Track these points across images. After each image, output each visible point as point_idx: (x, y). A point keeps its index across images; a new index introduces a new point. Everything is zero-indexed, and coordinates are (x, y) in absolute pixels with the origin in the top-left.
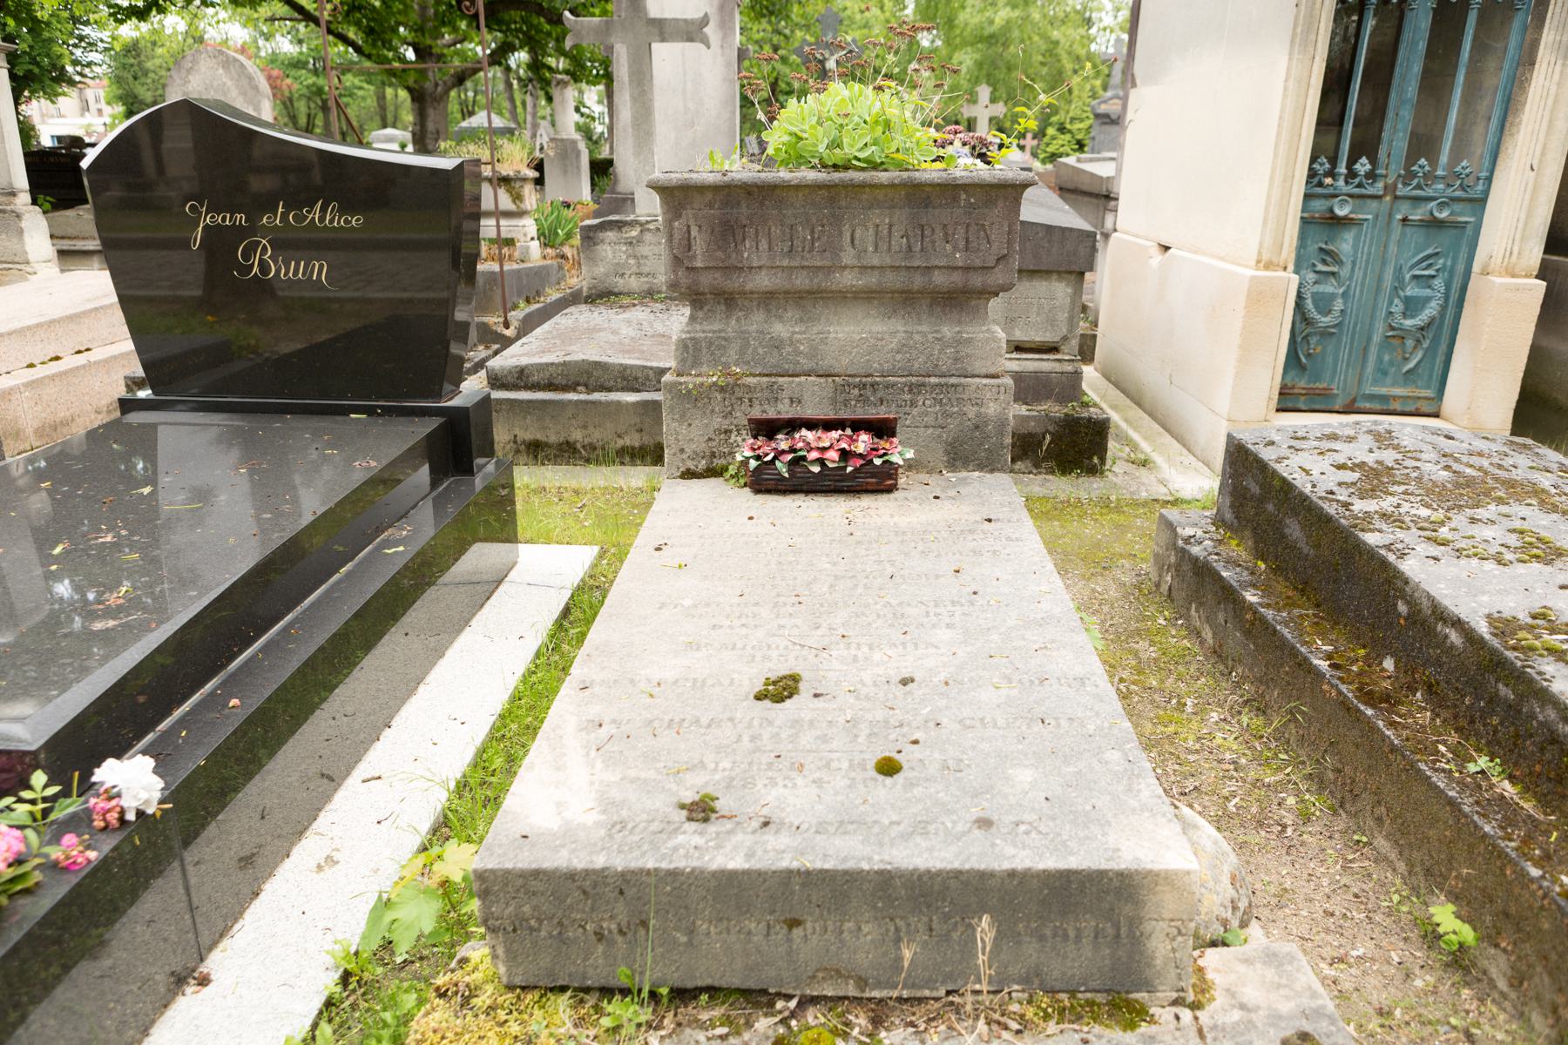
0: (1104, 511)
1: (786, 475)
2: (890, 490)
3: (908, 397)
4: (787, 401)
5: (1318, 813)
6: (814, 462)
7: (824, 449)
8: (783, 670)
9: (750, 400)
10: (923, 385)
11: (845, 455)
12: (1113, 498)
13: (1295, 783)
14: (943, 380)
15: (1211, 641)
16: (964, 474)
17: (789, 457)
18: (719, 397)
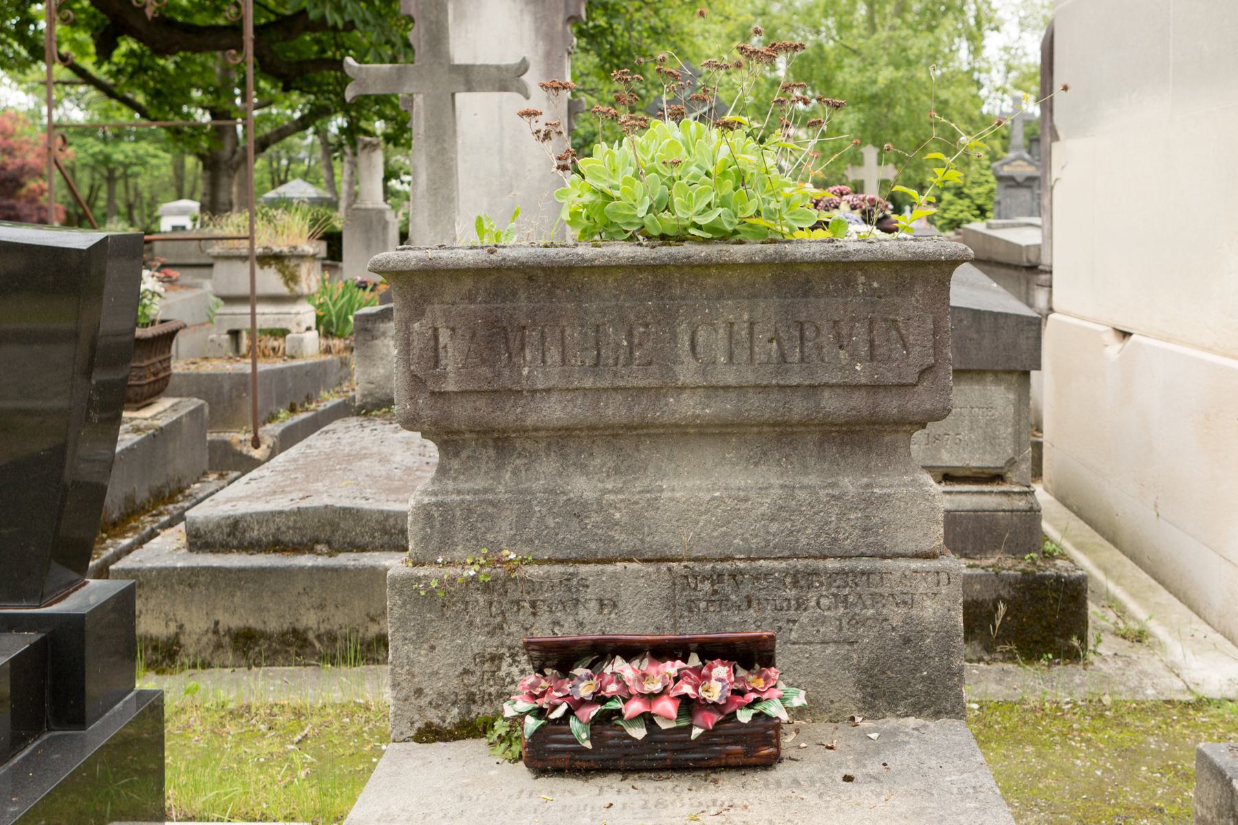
0: (1099, 723)
1: (588, 745)
2: (768, 764)
3: (791, 593)
4: (593, 604)
7: (652, 697)
9: (533, 604)
10: (816, 573)
11: (688, 706)
12: (1107, 700)
14: (847, 564)
16: (891, 722)
17: (593, 711)
18: (481, 599)
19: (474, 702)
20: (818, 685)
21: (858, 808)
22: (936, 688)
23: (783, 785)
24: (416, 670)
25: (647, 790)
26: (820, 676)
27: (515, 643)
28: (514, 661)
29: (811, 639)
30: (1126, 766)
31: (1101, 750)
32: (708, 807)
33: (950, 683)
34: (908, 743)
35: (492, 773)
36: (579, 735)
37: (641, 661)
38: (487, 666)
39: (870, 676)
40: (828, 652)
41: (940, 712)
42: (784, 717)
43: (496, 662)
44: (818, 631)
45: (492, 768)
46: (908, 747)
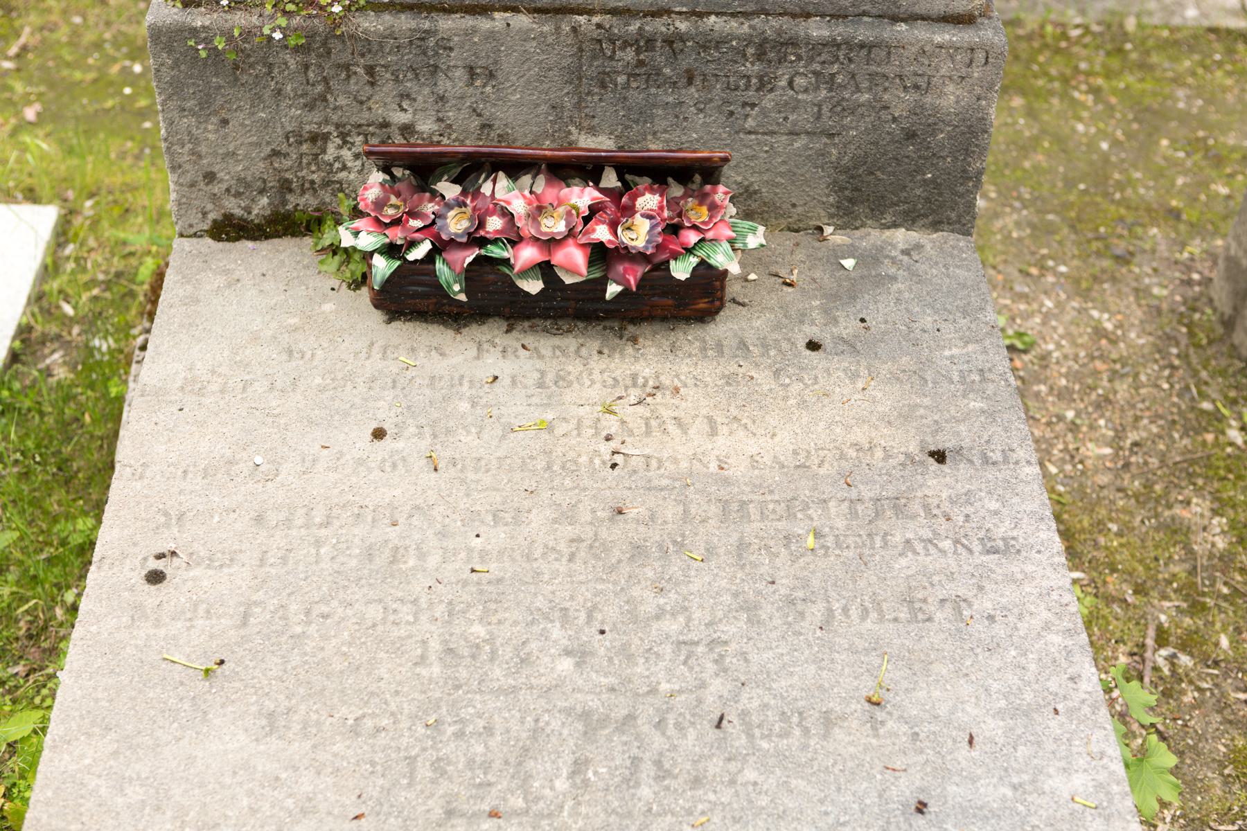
0: (1115, 63)
1: (463, 297)
2: (705, 316)
3: (753, 68)
4: (459, 73)
6: (524, 273)
7: (552, 243)
9: (370, 70)
10: (793, 43)
11: (600, 255)
12: (1131, 24)
14: (840, 31)
16: (872, 237)
17: (470, 256)
18: (292, 62)
19: (291, 190)
20: (778, 185)
21: (826, 401)
22: (941, 194)
23: (726, 350)
24: (203, 149)
25: (543, 352)
26: (782, 174)
27: (344, 120)
28: (345, 142)
29: (775, 128)
30: (1141, 137)
31: (1112, 108)
32: (626, 388)
33: (961, 189)
34: (894, 279)
35: (328, 307)
36: (449, 286)
37: (534, 177)
38: (305, 147)
39: (852, 177)
40: (796, 145)
41: (940, 222)
42: (734, 269)
43: (319, 143)
44: (786, 119)
45: (325, 298)
46: (895, 287)
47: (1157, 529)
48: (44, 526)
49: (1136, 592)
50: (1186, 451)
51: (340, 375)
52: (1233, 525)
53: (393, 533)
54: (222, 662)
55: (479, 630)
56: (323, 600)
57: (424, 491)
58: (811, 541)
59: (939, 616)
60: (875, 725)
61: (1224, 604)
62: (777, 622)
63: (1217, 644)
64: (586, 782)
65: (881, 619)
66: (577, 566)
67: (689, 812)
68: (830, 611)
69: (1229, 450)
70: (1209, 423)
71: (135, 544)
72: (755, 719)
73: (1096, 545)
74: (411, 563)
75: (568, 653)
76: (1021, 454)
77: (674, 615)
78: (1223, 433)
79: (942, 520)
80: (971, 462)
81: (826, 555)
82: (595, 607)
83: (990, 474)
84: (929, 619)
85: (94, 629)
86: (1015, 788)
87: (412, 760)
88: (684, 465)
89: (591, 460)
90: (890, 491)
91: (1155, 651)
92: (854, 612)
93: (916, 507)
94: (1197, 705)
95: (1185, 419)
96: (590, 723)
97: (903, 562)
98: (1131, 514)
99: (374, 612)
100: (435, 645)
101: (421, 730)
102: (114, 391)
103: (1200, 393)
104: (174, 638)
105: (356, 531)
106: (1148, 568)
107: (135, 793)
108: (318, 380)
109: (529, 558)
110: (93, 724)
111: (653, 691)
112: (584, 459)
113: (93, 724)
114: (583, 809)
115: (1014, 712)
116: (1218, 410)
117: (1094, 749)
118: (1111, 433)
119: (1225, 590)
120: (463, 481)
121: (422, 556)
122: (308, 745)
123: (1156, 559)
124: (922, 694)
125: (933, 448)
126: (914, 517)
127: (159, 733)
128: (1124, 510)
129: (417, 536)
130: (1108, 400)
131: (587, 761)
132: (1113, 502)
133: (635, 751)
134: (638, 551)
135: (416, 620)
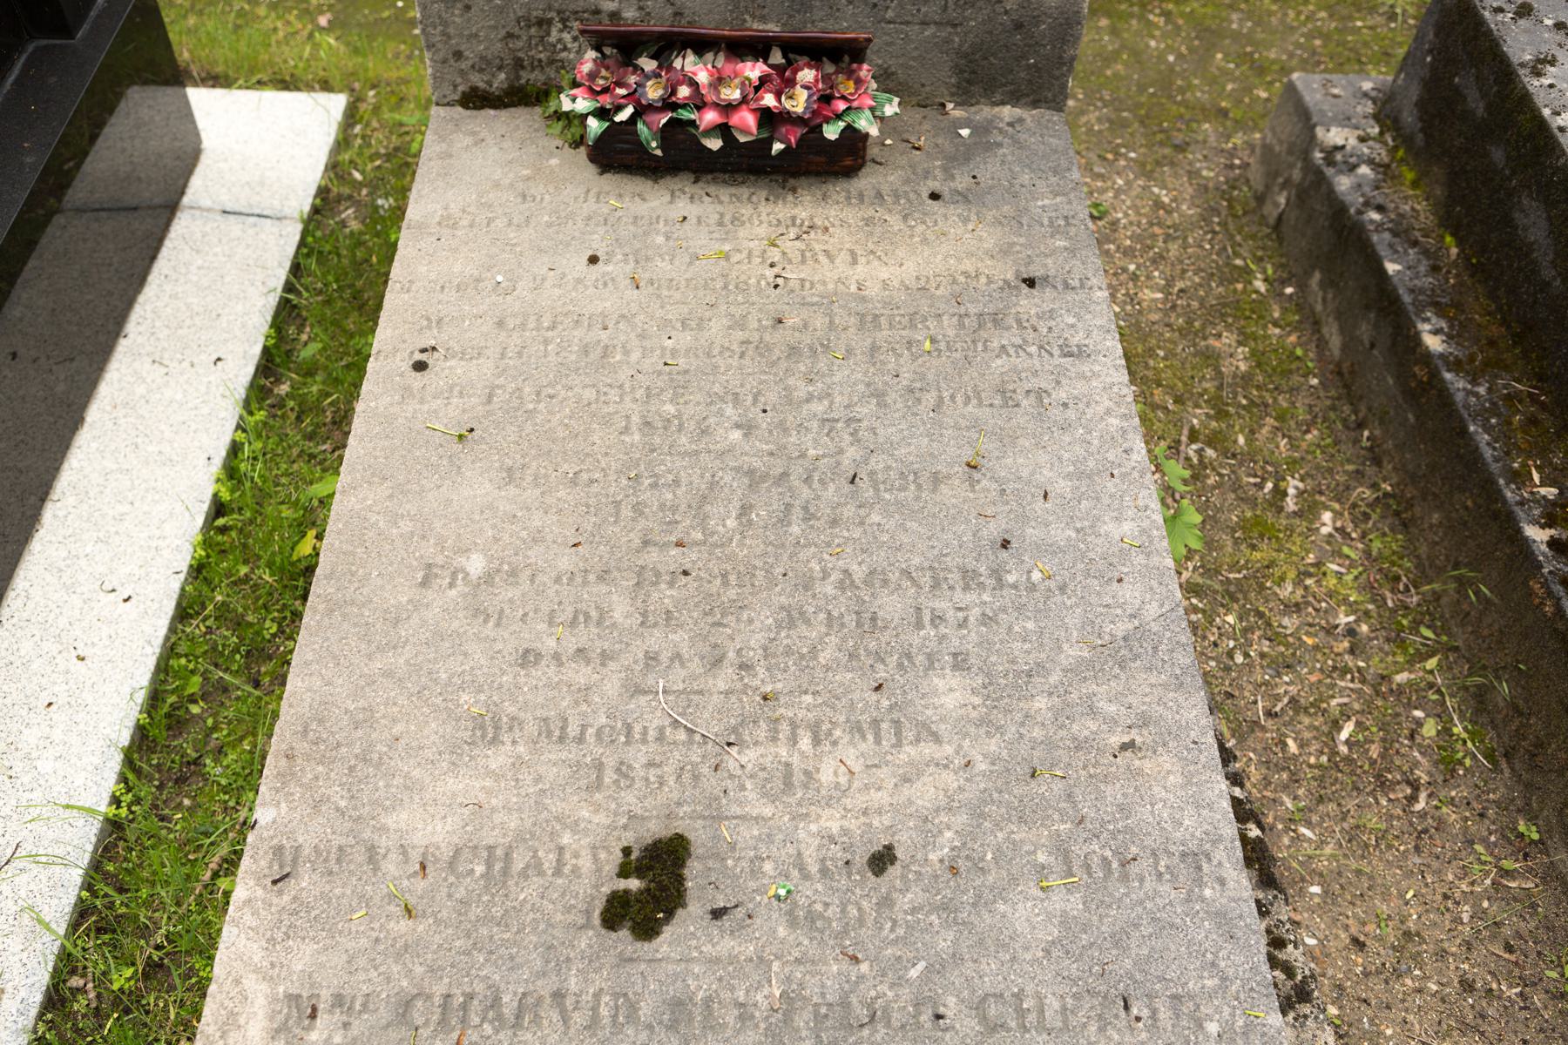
1: (659, 152)
2: (850, 172)
5: (1468, 762)
6: (709, 132)
7: (728, 108)
8: (655, 829)
13: (1439, 692)
15: (1337, 352)
16: (985, 112)
19: (523, 67)
20: (911, 67)
21: (943, 239)
22: (1040, 77)
23: (866, 199)
24: (451, 30)
25: (722, 198)
26: (914, 59)
27: (564, 7)
28: (565, 27)
29: (909, 18)
30: (1201, 52)
31: (1178, 28)
32: (787, 227)
33: (1057, 73)
34: (1000, 145)
35: (554, 162)
36: (648, 143)
37: (716, 55)
38: (533, 31)
39: (970, 62)
40: (926, 33)
41: (1039, 101)
42: (874, 131)
43: (545, 27)
44: (919, 10)
45: (551, 155)
46: (1001, 151)
47: (1195, 355)
48: (343, 341)
49: (1175, 402)
50: (1220, 296)
51: (563, 214)
52: (1253, 353)
53: (604, 335)
54: (472, 430)
55: (670, 409)
56: (550, 385)
57: (628, 304)
58: (927, 345)
59: (1025, 403)
60: (972, 483)
61: (1243, 412)
62: (899, 405)
63: (1235, 442)
64: (750, 522)
65: (980, 404)
66: (747, 361)
67: (828, 545)
68: (941, 398)
69: (1254, 296)
70: (1240, 276)
71: (404, 342)
72: (880, 477)
73: (1147, 366)
74: (618, 358)
75: (738, 426)
76: (1094, 281)
77: (820, 399)
78: (1250, 283)
79: (1030, 331)
80: (1055, 287)
81: (939, 356)
82: (759, 393)
83: (1070, 296)
84: (1017, 405)
85: (372, 404)
86: (1078, 531)
87: (617, 504)
88: (831, 286)
89: (759, 282)
90: (991, 308)
91: (1188, 445)
92: (959, 399)
93: (1011, 321)
94: (1218, 486)
95: (1222, 272)
96: (754, 479)
97: (999, 362)
98: (1175, 343)
99: (589, 394)
100: (636, 419)
101: (625, 482)
102: (393, 237)
103: (1234, 252)
104: (435, 411)
105: (576, 333)
106: (1186, 384)
107: (406, 526)
108: (546, 218)
109: (709, 355)
110: (373, 475)
111: (803, 455)
112: (753, 281)
113: (373, 475)
114: (748, 542)
115: (1080, 475)
116: (1247, 265)
117: (1141, 503)
118: (1163, 282)
119: (1244, 402)
120: (659, 296)
121: (626, 353)
122: (538, 492)
123: (1193, 378)
124: (1009, 461)
125: (1025, 276)
126: (1009, 328)
127: (424, 482)
128: (1170, 341)
129: (623, 338)
130: (1162, 257)
131: (751, 506)
132: (1161, 334)
133: (787, 500)
134: (793, 351)
135: (622, 400)
